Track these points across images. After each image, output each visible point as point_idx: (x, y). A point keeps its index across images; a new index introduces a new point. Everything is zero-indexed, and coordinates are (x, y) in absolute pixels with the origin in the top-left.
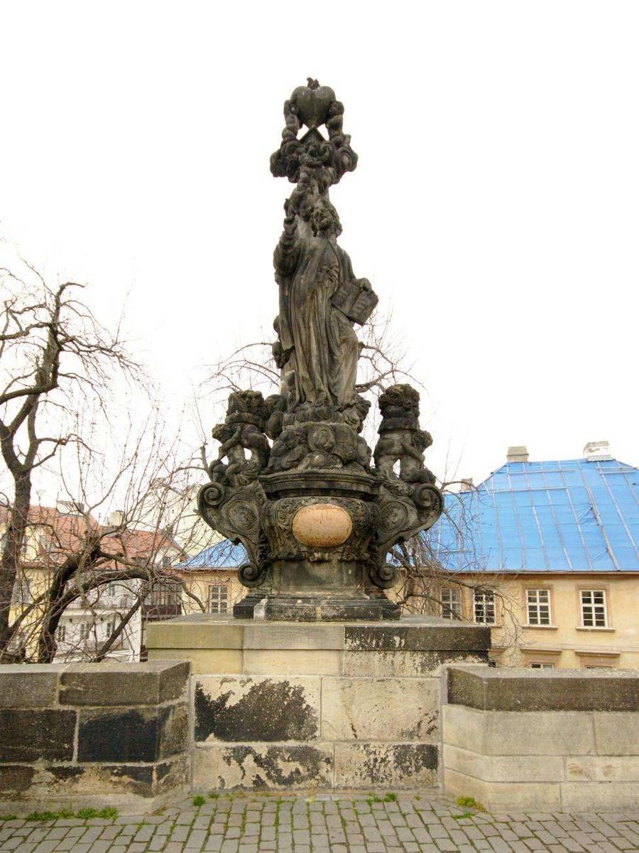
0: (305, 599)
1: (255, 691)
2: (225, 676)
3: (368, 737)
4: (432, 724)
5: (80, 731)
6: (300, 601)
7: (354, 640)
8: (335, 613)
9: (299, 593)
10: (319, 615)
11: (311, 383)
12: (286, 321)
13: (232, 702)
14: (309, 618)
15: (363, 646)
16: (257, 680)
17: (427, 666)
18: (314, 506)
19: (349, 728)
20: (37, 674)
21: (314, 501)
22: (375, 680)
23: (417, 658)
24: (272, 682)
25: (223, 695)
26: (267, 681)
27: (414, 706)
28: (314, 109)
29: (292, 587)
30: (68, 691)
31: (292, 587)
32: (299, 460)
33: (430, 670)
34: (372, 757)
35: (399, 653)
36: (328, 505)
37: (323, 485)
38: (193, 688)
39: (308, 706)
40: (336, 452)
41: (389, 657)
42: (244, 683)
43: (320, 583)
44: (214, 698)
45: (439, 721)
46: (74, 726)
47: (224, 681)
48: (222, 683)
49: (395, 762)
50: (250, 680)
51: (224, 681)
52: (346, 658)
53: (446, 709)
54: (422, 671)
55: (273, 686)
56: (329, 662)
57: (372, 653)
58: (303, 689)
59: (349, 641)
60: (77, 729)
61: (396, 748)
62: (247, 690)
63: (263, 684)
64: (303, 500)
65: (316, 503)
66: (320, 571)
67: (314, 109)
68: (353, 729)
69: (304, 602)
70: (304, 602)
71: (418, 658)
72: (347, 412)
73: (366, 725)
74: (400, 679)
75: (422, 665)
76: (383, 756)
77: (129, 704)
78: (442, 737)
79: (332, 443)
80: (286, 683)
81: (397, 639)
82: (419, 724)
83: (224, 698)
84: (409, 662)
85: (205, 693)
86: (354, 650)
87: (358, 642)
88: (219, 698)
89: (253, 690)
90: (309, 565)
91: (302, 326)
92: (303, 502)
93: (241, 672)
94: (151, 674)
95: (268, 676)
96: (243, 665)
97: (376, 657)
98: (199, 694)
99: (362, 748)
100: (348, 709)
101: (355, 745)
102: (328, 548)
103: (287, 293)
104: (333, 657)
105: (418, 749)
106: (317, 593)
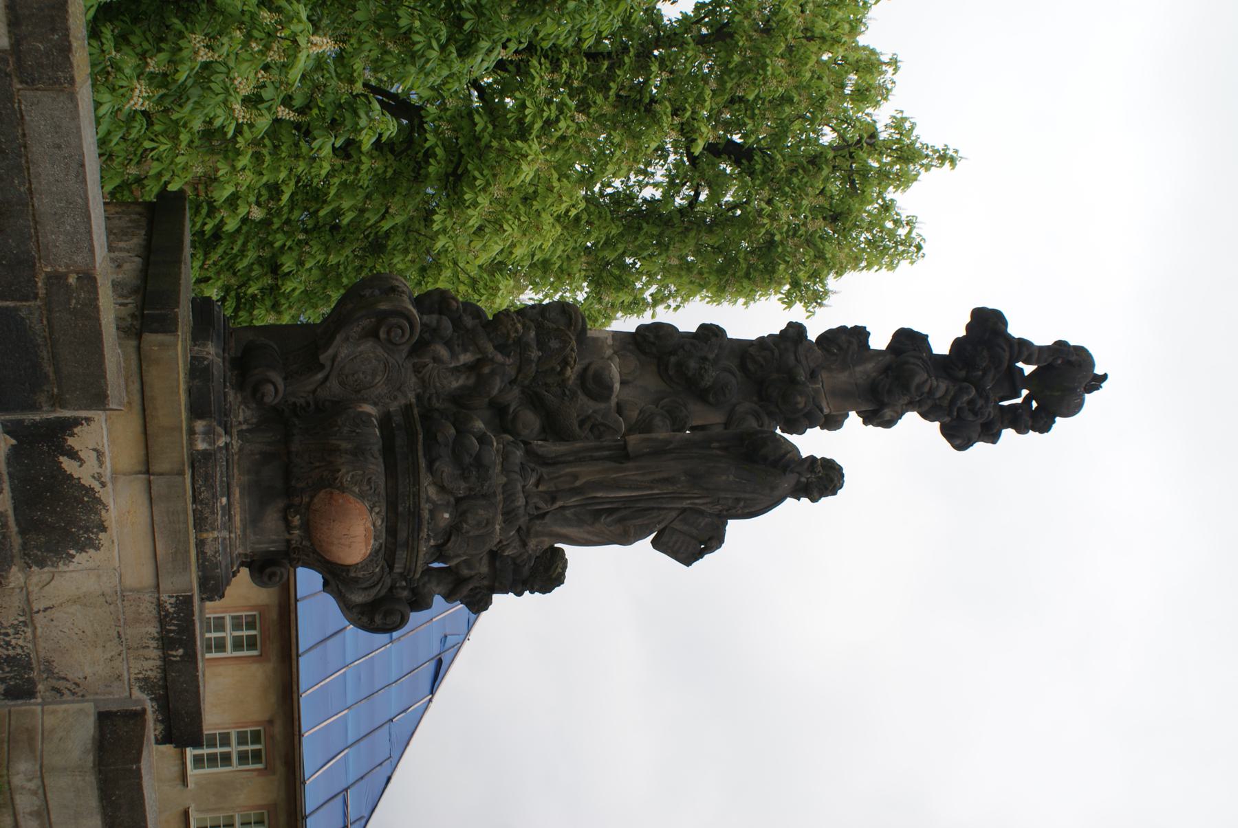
0: (228, 509)
1: (87, 492)
2: (107, 453)
3: (38, 626)
4: (65, 691)
5: (7, 308)
6: (224, 500)
7: (175, 605)
8: (209, 553)
9: (237, 493)
10: (205, 535)
11: (567, 486)
12: (672, 446)
13: (67, 464)
14: (200, 523)
15: (166, 616)
16: (102, 493)
17: (146, 684)
18: (369, 525)
19: (49, 604)
20: (91, 239)
21: (379, 522)
22: (121, 629)
23: (155, 673)
24: (103, 513)
25: (77, 453)
26: (105, 506)
27: (88, 671)
28: (1064, 379)
29: (245, 479)
30: (68, 286)
31: (245, 479)
32: (442, 489)
33: (140, 688)
34: (11, 631)
35: (160, 653)
36: (372, 541)
37: (402, 535)
38: (83, 414)
39: (73, 556)
40: (453, 538)
41: (153, 644)
42: (98, 477)
43: (254, 520)
44: (71, 441)
45: (71, 698)
46: (13, 300)
47: (100, 454)
48: (95, 450)
49: (8, 656)
50: (103, 485)
51: (100, 454)
52: (148, 599)
53: (90, 707)
54: (137, 679)
55: (97, 513)
56: (139, 574)
57: (158, 625)
58: (98, 549)
59: (173, 600)
60: (10, 304)
61: (28, 655)
62: (87, 481)
63: (99, 501)
64: (382, 508)
65: (374, 525)
66: (272, 520)
67: (1064, 379)
68: (46, 610)
69: (223, 508)
70: (223, 508)
71: (154, 674)
72: (517, 543)
73: (55, 623)
74: (124, 655)
75: (146, 679)
76: (13, 642)
77: (57, 371)
78: (50, 703)
79: (467, 532)
80: (104, 529)
81: (181, 651)
82: (64, 679)
83: (73, 455)
84: (149, 663)
85: (76, 430)
86: (160, 605)
87: (171, 610)
88: (72, 448)
89: (90, 491)
90: (281, 504)
91: (656, 476)
92: (377, 510)
93: (115, 474)
94: (106, 396)
95: (112, 506)
96: (124, 474)
97: (153, 630)
98: (77, 422)
99: (22, 619)
100: (75, 601)
101: (23, 610)
102: (307, 527)
103: (715, 445)
104: (147, 578)
105: (29, 679)
106: (238, 518)
